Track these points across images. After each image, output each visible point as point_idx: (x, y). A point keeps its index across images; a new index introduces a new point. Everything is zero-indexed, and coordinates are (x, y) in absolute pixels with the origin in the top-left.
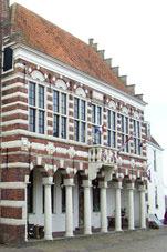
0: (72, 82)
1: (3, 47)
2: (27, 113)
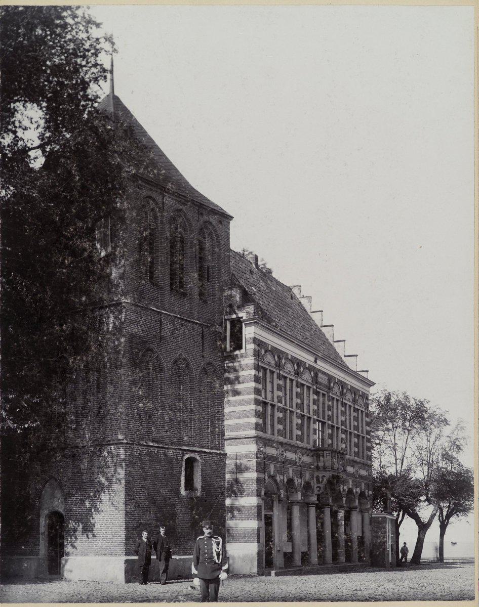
0: (300, 363)
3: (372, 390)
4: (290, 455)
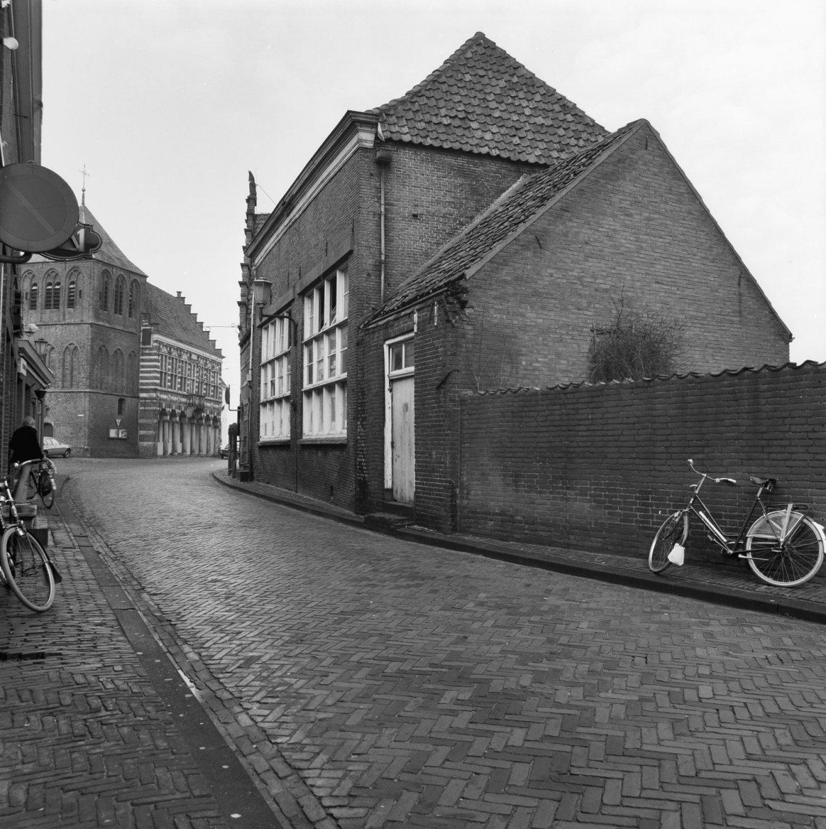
2: (159, 375)
4: (175, 398)
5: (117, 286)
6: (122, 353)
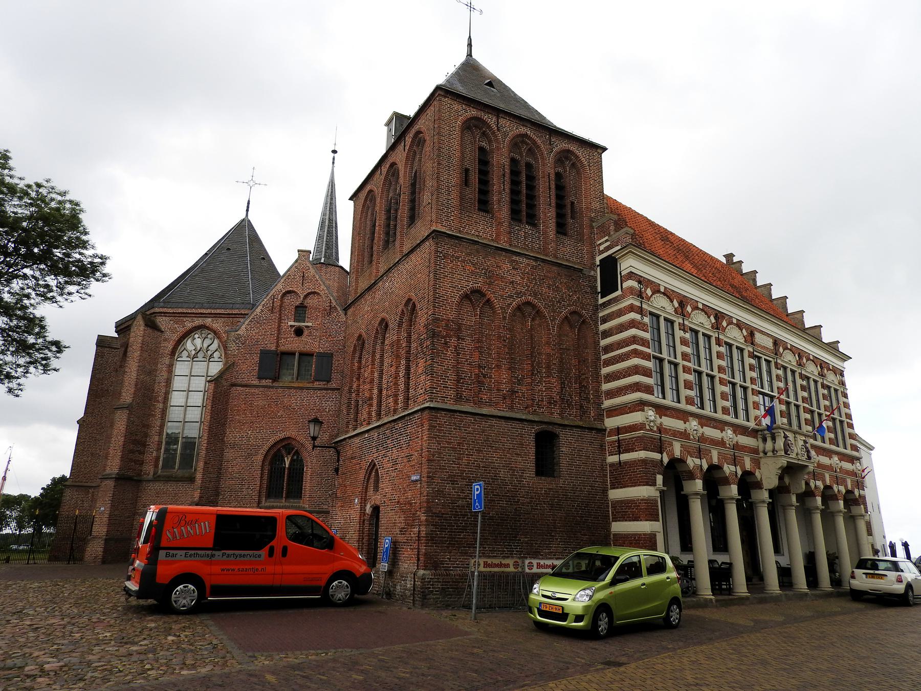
0: (719, 316)
1: (598, 259)
2: (649, 364)
3: (847, 364)
5: (513, 161)
6: (539, 312)
